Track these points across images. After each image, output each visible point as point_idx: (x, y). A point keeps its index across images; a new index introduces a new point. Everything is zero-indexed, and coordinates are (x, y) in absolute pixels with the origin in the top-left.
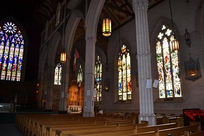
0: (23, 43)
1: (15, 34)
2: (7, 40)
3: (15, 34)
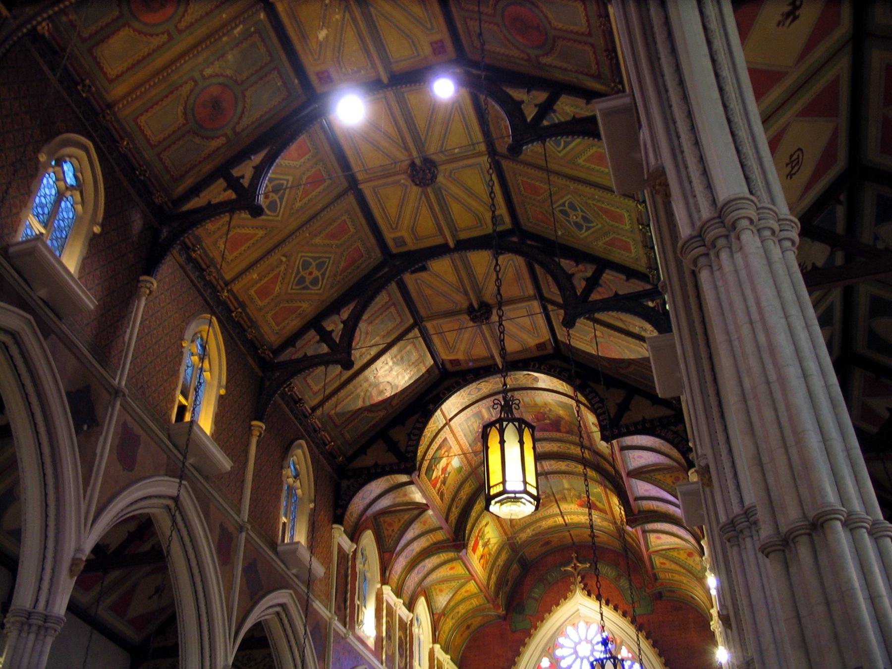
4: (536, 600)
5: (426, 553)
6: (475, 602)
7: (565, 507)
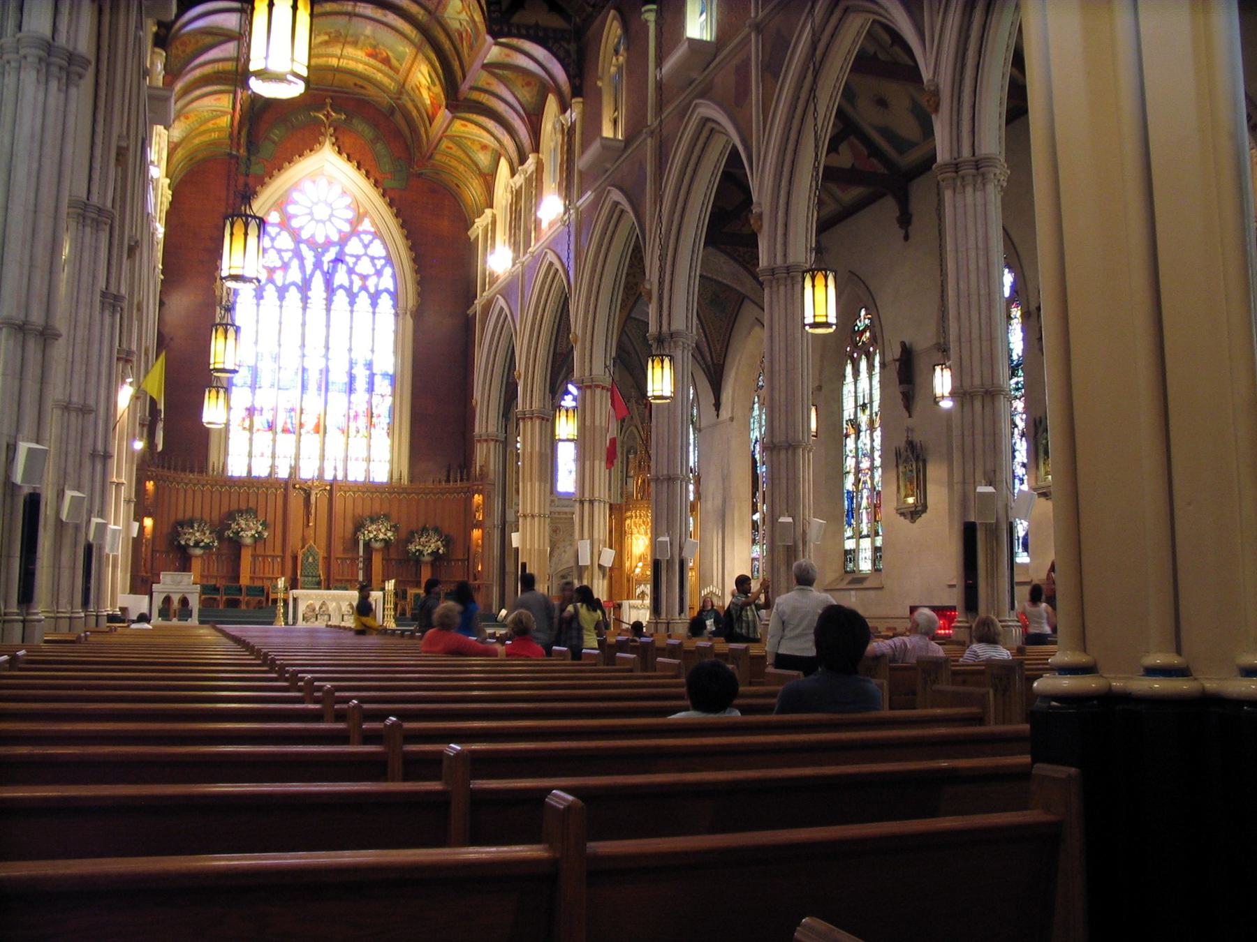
0: (387, 282)
1: (344, 240)
2: (312, 275)
3: (344, 240)
4: (274, 142)
5: (205, 80)
6: (214, 135)
7: (350, 51)
